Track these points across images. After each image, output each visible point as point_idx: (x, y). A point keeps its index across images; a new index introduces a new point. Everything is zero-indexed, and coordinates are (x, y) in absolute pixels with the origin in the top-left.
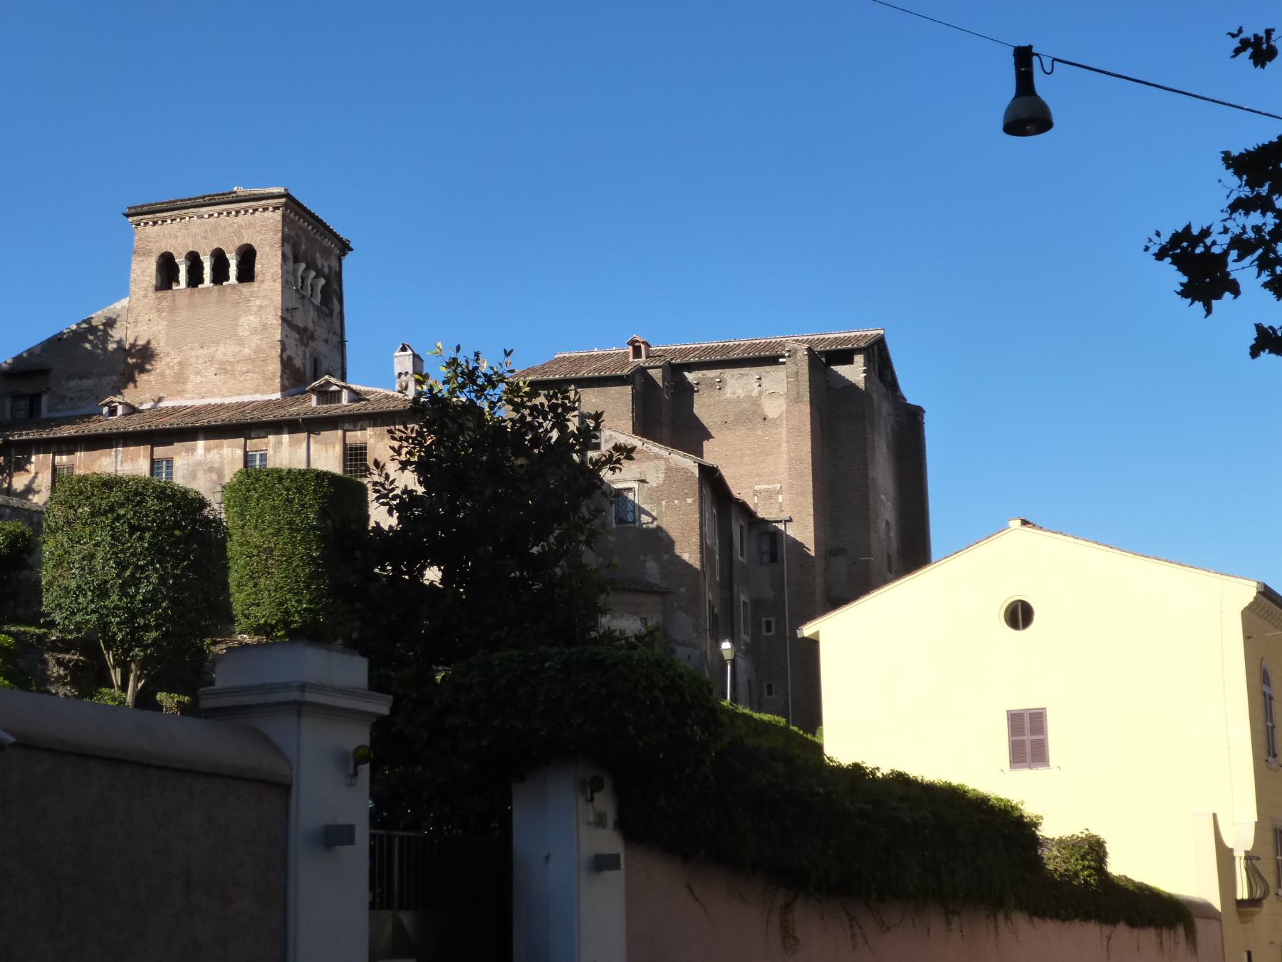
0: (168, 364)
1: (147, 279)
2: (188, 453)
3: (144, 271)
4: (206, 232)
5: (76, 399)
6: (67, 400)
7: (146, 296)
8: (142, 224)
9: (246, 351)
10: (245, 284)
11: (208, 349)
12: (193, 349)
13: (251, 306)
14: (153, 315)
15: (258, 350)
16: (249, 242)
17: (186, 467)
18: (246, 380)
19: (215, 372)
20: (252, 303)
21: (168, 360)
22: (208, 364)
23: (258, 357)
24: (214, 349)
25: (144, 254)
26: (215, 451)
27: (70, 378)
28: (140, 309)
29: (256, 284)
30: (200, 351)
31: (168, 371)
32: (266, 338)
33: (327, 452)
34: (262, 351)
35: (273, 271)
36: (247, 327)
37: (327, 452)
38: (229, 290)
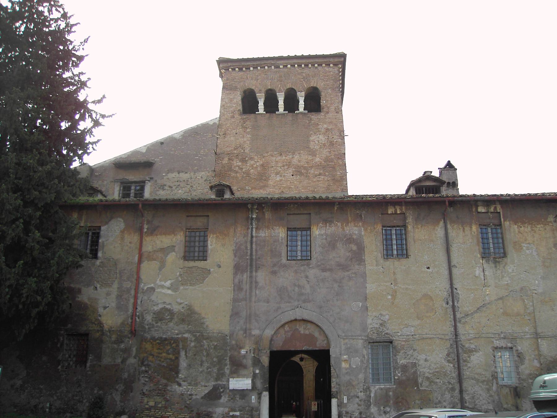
0: (252, 166)
1: (234, 105)
2: (326, 224)
3: (231, 100)
4: (281, 77)
5: (174, 188)
6: (166, 188)
7: (233, 117)
8: (230, 70)
9: (317, 159)
10: (313, 113)
11: (285, 156)
12: (273, 156)
13: (319, 128)
14: (240, 130)
15: (327, 160)
16: (315, 86)
17: (325, 237)
18: (318, 181)
19: (292, 174)
20: (320, 126)
21: (252, 162)
22: (286, 167)
23: (328, 165)
24: (291, 157)
25: (231, 89)
26: (352, 224)
27: (170, 171)
28: (228, 125)
29: (322, 114)
30: (279, 158)
31: (252, 171)
32: (334, 151)
33: (464, 231)
34: (332, 161)
35: (336, 105)
36: (317, 142)
37: (464, 231)
38: (301, 116)
